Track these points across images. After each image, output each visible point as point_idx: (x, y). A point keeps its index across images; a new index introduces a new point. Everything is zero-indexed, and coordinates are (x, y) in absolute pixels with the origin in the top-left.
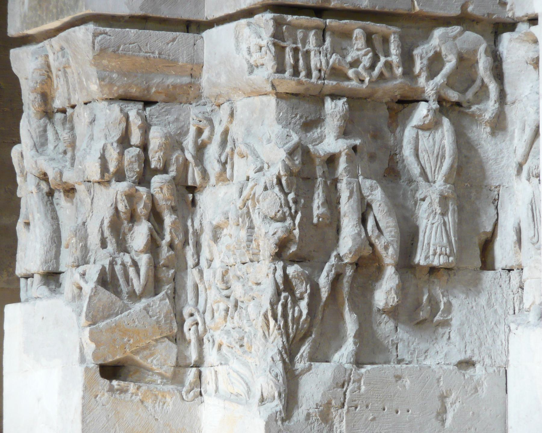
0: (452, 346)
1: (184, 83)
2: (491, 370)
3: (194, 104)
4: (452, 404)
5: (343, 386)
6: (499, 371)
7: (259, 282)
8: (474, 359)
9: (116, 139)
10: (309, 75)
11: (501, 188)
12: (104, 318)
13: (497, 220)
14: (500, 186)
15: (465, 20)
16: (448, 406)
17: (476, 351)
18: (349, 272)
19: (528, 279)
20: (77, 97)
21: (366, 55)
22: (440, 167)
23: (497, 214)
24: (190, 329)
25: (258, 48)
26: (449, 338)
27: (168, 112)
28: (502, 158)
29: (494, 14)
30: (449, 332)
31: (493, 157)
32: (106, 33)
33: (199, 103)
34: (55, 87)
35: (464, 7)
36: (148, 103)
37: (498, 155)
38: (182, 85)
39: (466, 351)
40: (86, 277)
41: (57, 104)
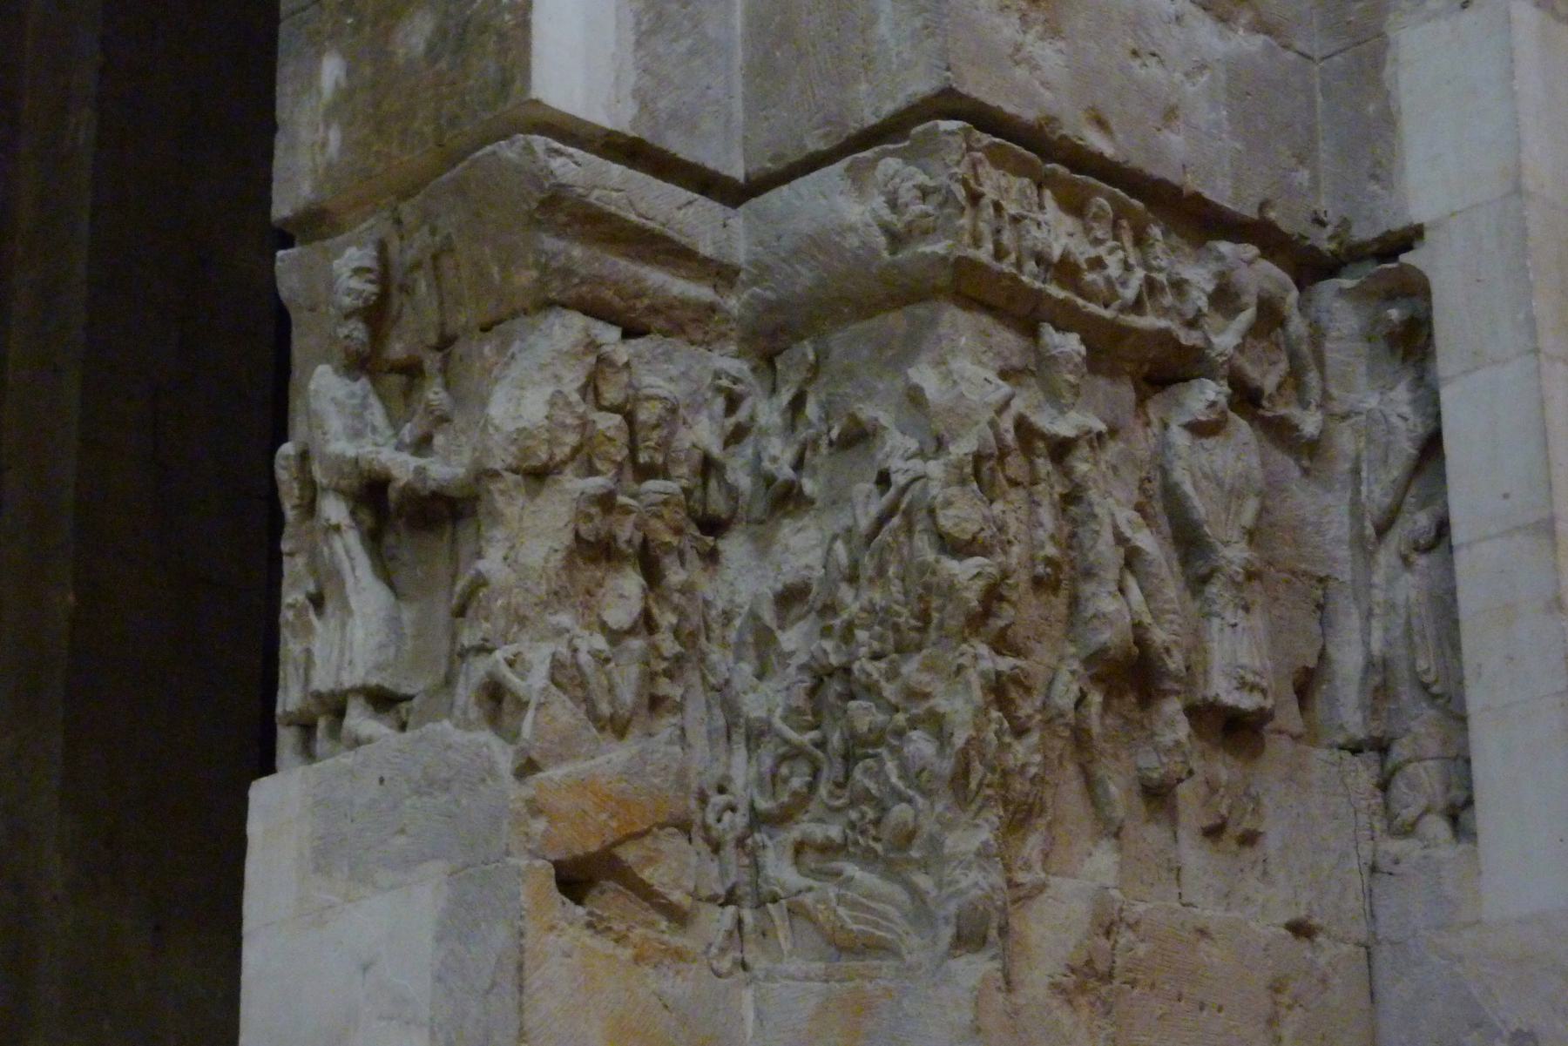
5: (1108, 934)
7: (928, 690)
8: (1316, 921)
9: (577, 384)
10: (1019, 265)
12: (561, 759)
13: (1324, 648)
14: (1328, 577)
15: (1264, 236)
16: (1283, 1011)
18: (1096, 698)
19: (1409, 761)
20: (462, 319)
21: (1111, 252)
22: (1238, 514)
24: (719, 820)
25: (919, 194)
27: (669, 358)
31: (1313, 519)
32: (570, 156)
34: (394, 313)
35: (1263, 206)
36: (630, 333)
40: (518, 667)
41: (397, 349)
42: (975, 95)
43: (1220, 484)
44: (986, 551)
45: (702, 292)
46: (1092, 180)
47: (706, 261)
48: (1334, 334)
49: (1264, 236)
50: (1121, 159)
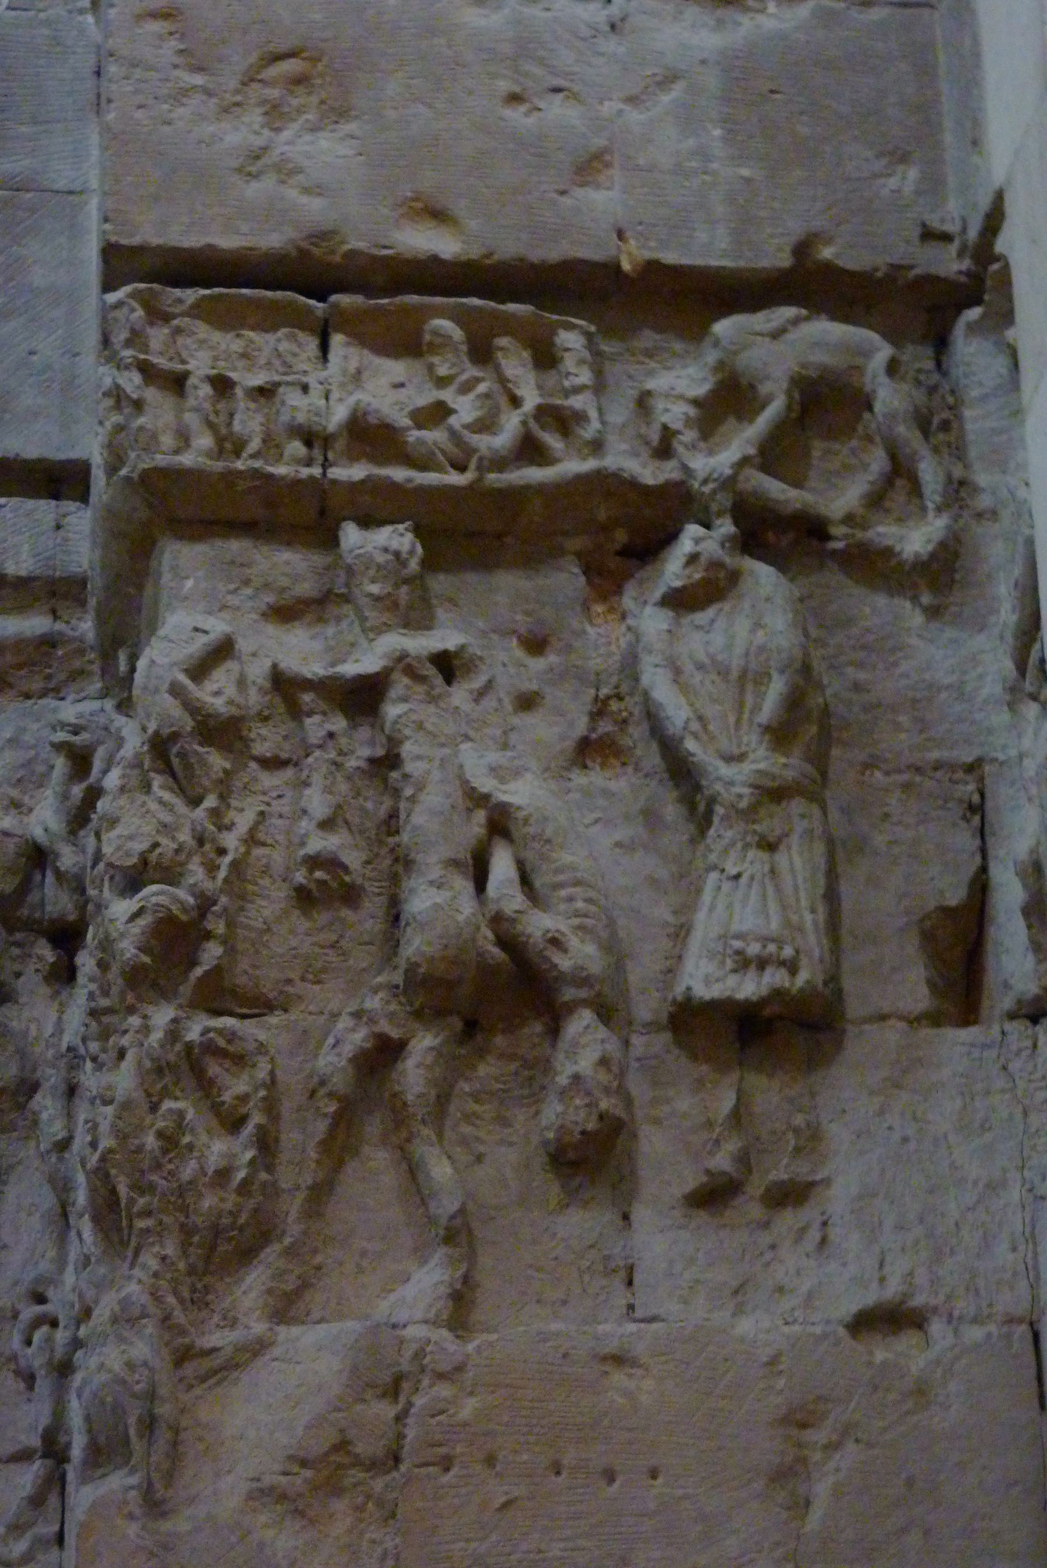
0: (833, 1266)
1: (28, 633)
2: (975, 1334)
3: (71, 697)
4: (832, 1447)
6: (1008, 1336)
8: (918, 1300)
11: (987, 768)
13: (984, 869)
14: (979, 762)
15: (808, 283)
17: (922, 1277)
22: (757, 708)
23: (983, 851)
24: (29, 1343)
26: (824, 1241)
28: (981, 677)
29: (911, 267)
30: (825, 1224)
33: (83, 695)
37: (965, 673)
38: (22, 641)
39: (882, 1280)
42: (155, 241)
43: (723, 672)
44: (170, 875)
45: (35, 624)
46: (414, 299)
47: (23, 583)
48: (975, 393)
49: (808, 283)
50: (474, 252)
